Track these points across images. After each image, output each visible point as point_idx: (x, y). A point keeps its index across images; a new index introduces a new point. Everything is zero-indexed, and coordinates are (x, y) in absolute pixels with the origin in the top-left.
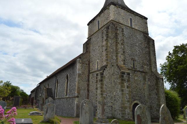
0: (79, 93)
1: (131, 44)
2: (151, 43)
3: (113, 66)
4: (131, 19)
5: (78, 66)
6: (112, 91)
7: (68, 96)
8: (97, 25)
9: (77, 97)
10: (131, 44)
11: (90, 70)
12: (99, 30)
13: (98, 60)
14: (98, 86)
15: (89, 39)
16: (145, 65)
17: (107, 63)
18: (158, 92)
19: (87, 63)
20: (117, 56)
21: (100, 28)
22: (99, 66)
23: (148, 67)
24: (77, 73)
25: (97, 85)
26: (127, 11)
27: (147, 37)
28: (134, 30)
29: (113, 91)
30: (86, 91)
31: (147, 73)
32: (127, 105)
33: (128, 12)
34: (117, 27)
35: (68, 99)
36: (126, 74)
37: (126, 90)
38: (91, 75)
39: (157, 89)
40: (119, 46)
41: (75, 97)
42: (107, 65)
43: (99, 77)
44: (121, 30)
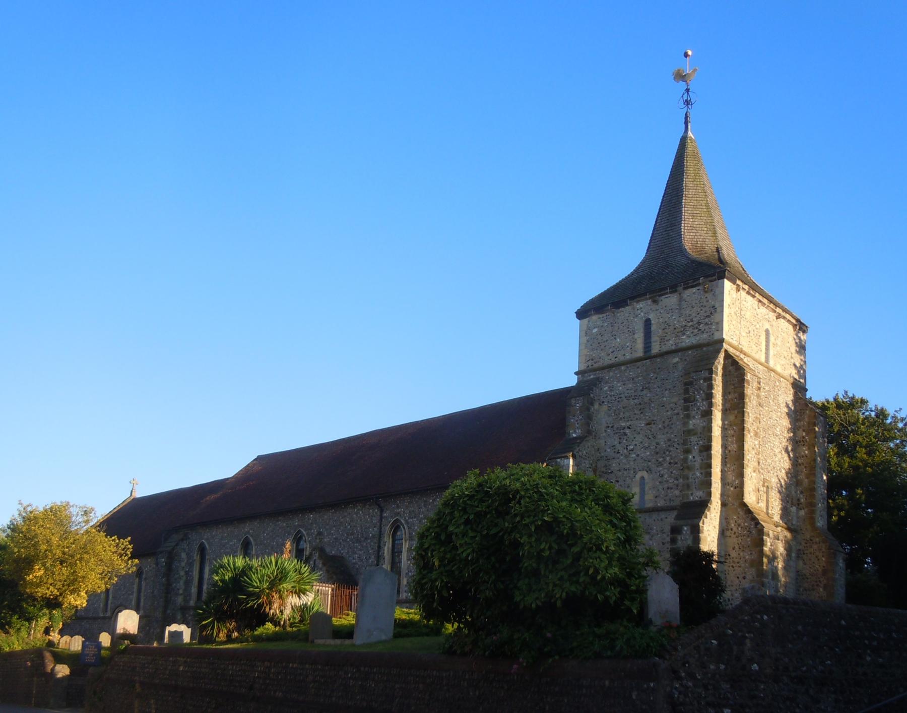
12: (648, 355)
13: (645, 474)
16: (792, 504)
21: (656, 349)
23: (802, 513)
28: (773, 374)
40: (750, 442)
44: (755, 384)
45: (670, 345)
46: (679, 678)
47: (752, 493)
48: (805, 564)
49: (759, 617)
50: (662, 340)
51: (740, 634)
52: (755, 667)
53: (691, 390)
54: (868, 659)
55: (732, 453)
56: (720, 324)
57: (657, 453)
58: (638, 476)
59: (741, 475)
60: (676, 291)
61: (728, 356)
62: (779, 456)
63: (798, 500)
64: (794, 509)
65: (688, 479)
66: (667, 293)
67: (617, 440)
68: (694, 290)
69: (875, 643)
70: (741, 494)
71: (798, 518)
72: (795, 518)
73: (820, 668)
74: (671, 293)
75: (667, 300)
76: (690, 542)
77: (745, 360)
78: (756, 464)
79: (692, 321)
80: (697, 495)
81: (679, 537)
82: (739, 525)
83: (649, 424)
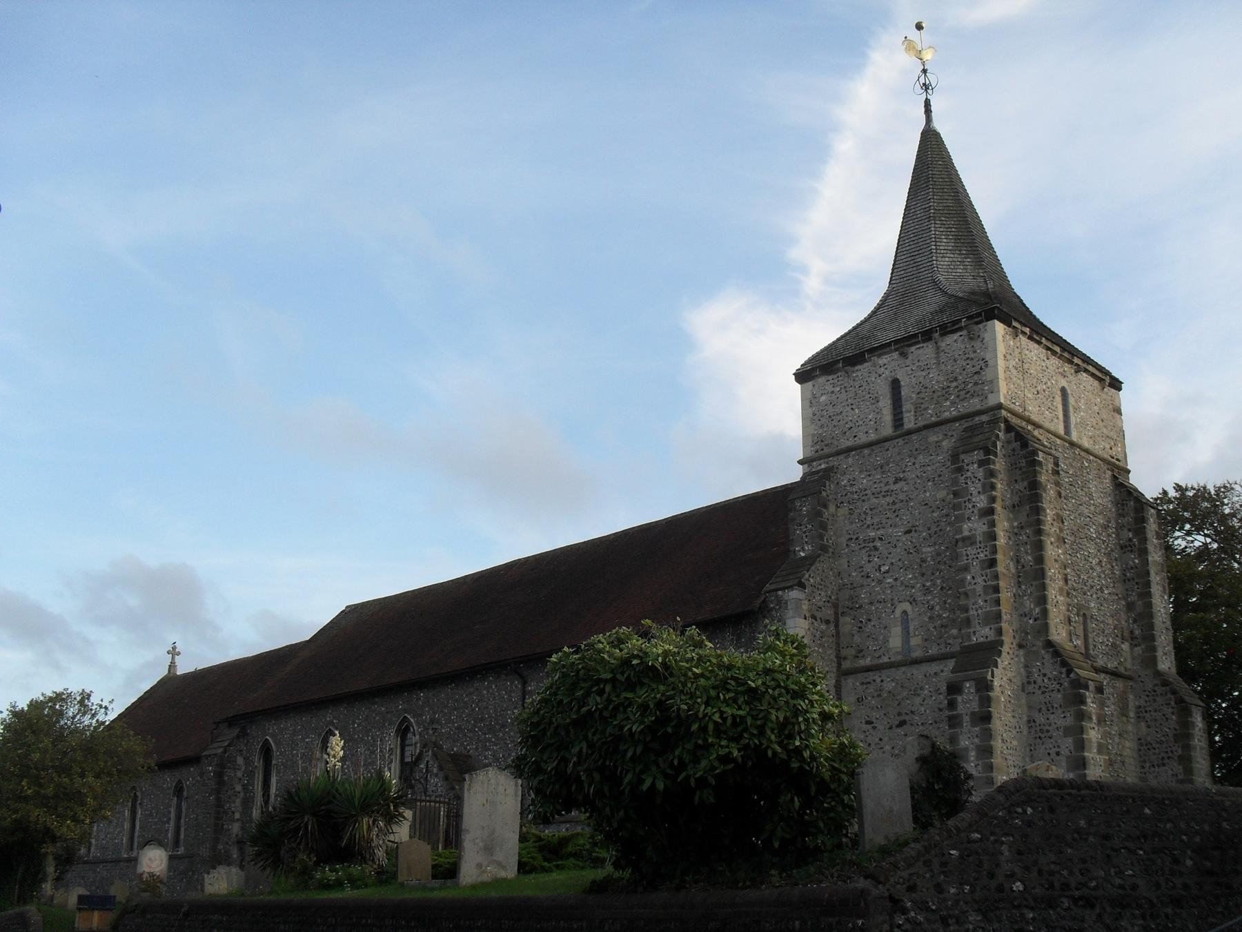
8: (886, 404)
23: (1138, 650)
26: (1048, 349)
31: (1130, 678)
33: (1054, 353)
36: (1091, 685)
44: (1051, 466)
45: (930, 415)
46: (904, 911)
47: (1060, 626)
49: (1020, 810)
50: (919, 409)
51: (992, 838)
52: (1018, 886)
53: (962, 479)
54: (1189, 863)
55: (1028, 568)
56: (993, 382)
57: (923, 575)
58: (898, 612)
59: (1042, 600)
60: (930, 339)
61: (1009, 428)
62: (1098, 569)
63: (1132, 632)
64: (1125, 647)
65: (967, 610)
66: (918, 342)
67: (866, 558)
68: (955, 336)
69: (1198, 839)
71: (1133, 658)
72: (1129, 660)
73: (1118, 881)
74: (924, 341)
75: (921, 351)
76: (975, 706)
77: (1036, 433)
78: (1061, 583)
79: (956, 379)
81: (959, 699)
82: (1045, 675)
83: (909, 532)
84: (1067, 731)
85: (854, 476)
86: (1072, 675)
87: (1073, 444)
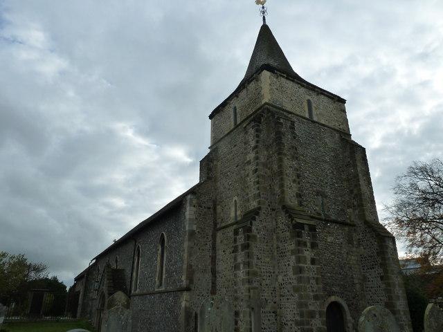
0: (190, 279)
1: (313, 159)
2: (358, 156)
3: (273, 210)
4: (309, 102)
5: (189, 212)
6: (274, 273)
7: (163, 289)
8: (232, 117)
9: (188, 289)
10: (313, 159)
11: (219, 221)
12: (237, 126)
13: (236, 198)
14: (239, 260)
15: (214, 148)
16: (349, 207)
17: (259, 203)
18: (386, 271)
19: (210, 204)
20: (282, 186)
22: (238, 213)
24: (187, 229)
25: (235, 259)
26: (299, 84)
27: (347, 141)
28: (317, 125)
29: (276, 273)
30: (208, 276)
32: (314, 306)
33: (303, 86)
34: (278, 118)
35: (164, 297)
36: (306, 228)
37: (311, 271)
38: (219, 234)
39: (384, 265)
40: (287, 162)
41: (182, 290)
42: (259, 208)
43: (241, 239)
48: (365, 249)
70: (282, 200)
80: (254, 204)
84: (293, 252)
85: (224, 148)
86: (294, 222)
87: (314, 122)
